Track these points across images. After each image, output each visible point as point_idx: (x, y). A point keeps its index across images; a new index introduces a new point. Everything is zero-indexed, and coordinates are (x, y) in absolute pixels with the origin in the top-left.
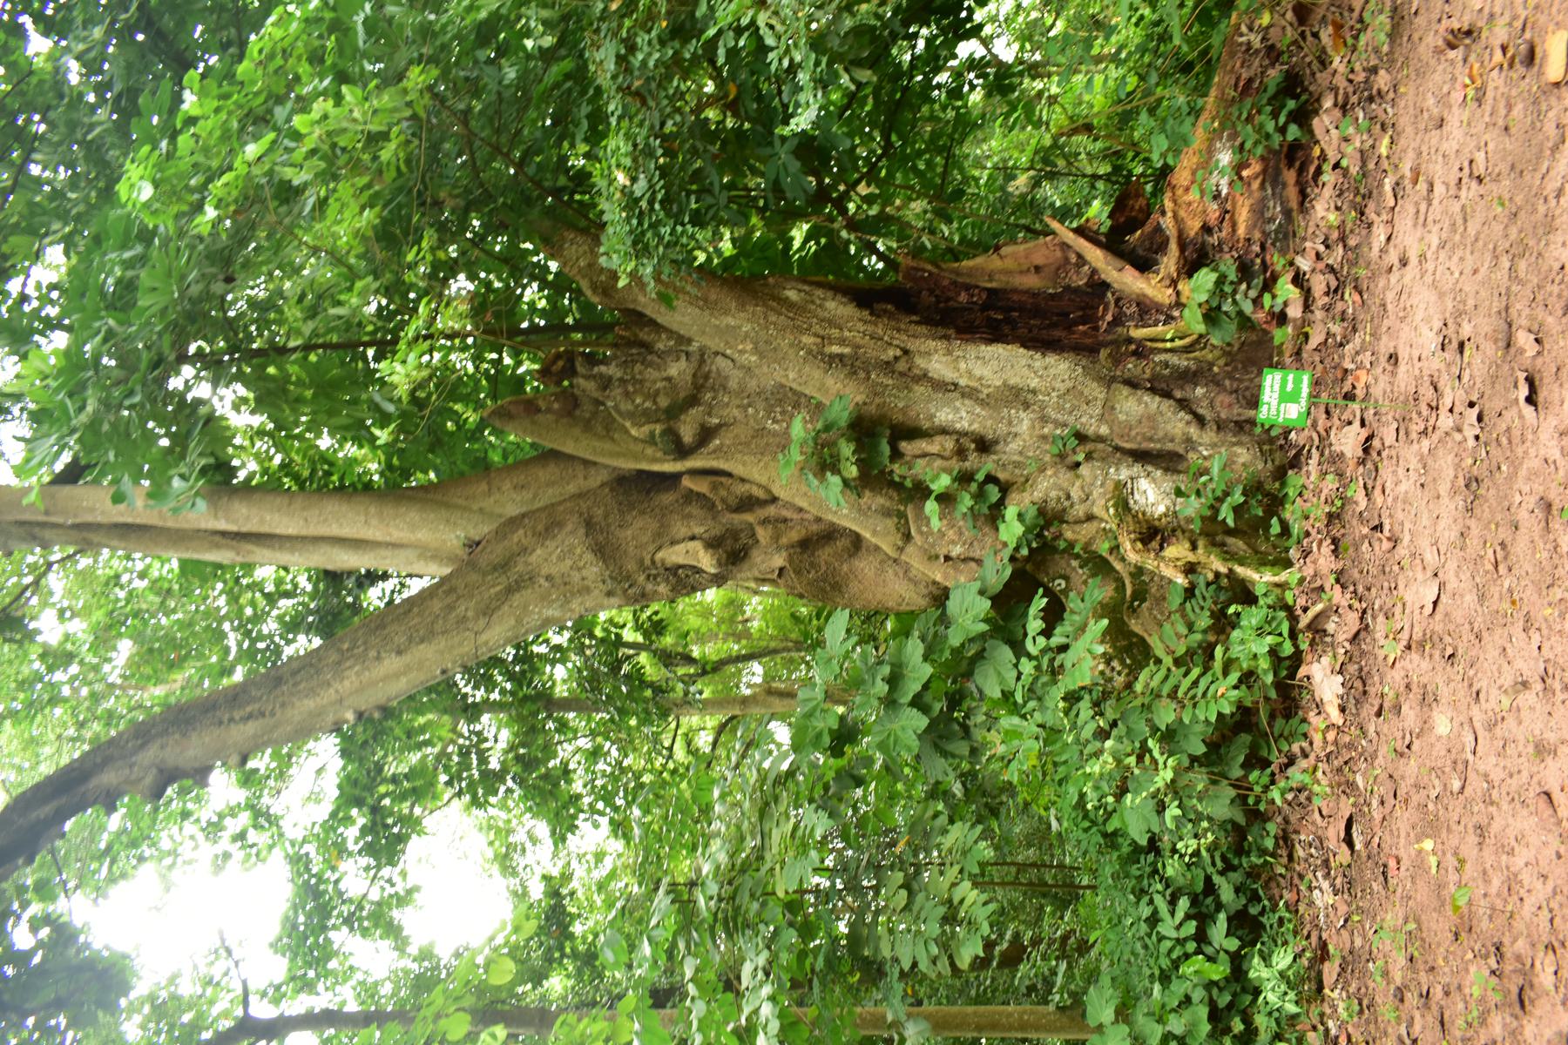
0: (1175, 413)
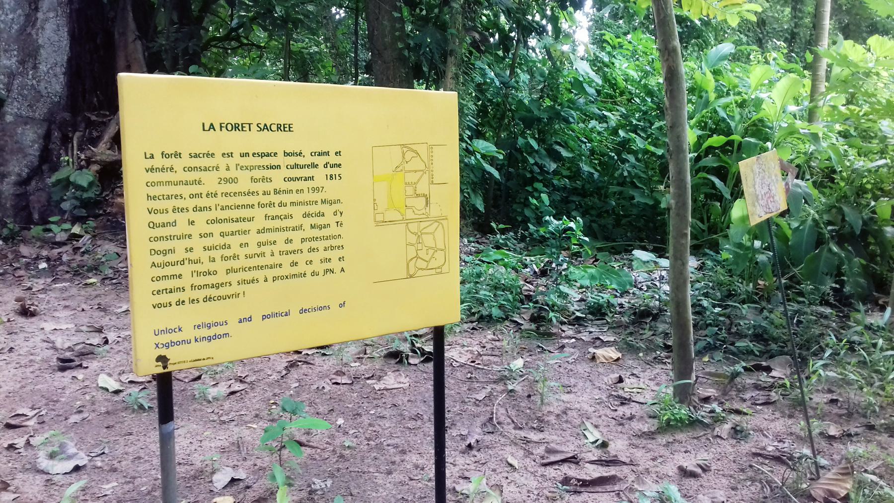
0: (27, 166)
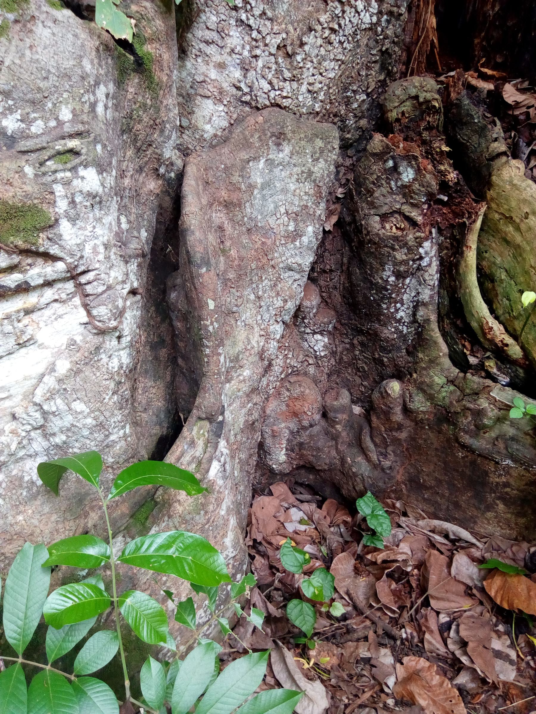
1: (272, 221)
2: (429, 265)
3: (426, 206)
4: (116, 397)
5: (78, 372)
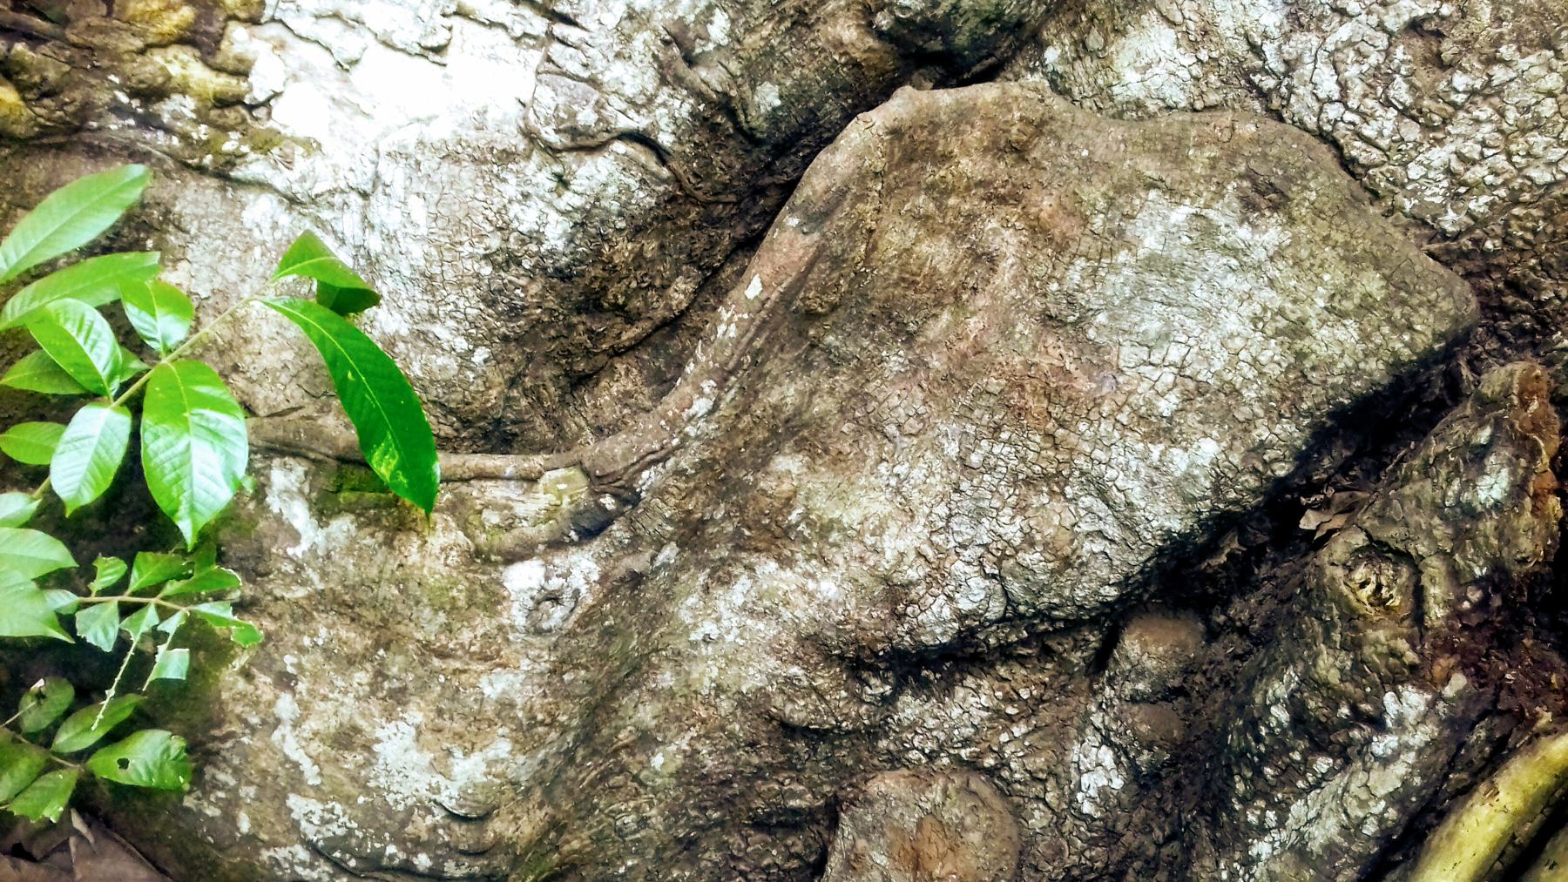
0: (998, 563)
1: (1128, 355)
2: (1386, 761)
3: (1475, 595)
4: (487, 270)
5: (452, 157)
